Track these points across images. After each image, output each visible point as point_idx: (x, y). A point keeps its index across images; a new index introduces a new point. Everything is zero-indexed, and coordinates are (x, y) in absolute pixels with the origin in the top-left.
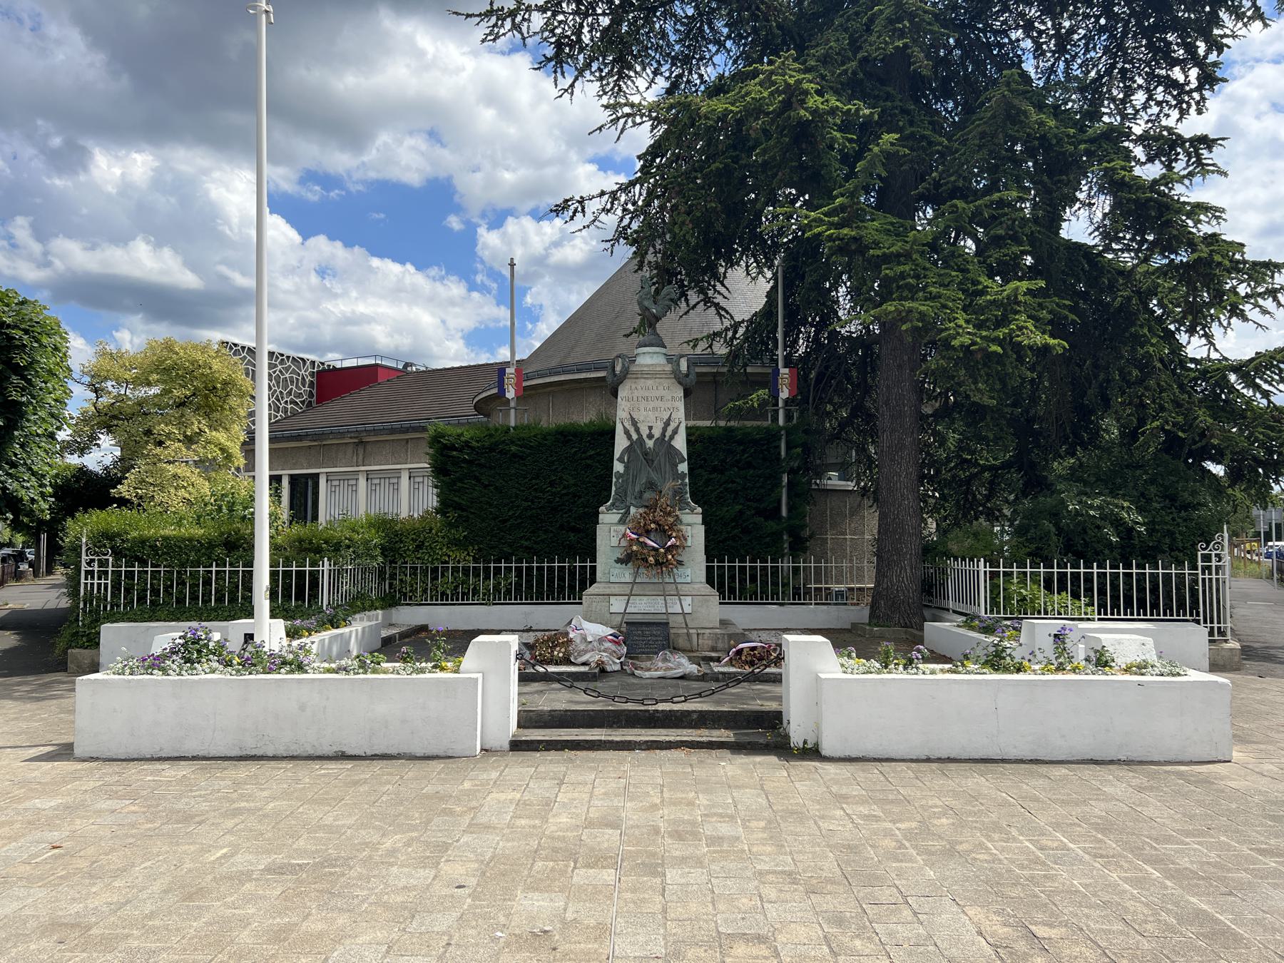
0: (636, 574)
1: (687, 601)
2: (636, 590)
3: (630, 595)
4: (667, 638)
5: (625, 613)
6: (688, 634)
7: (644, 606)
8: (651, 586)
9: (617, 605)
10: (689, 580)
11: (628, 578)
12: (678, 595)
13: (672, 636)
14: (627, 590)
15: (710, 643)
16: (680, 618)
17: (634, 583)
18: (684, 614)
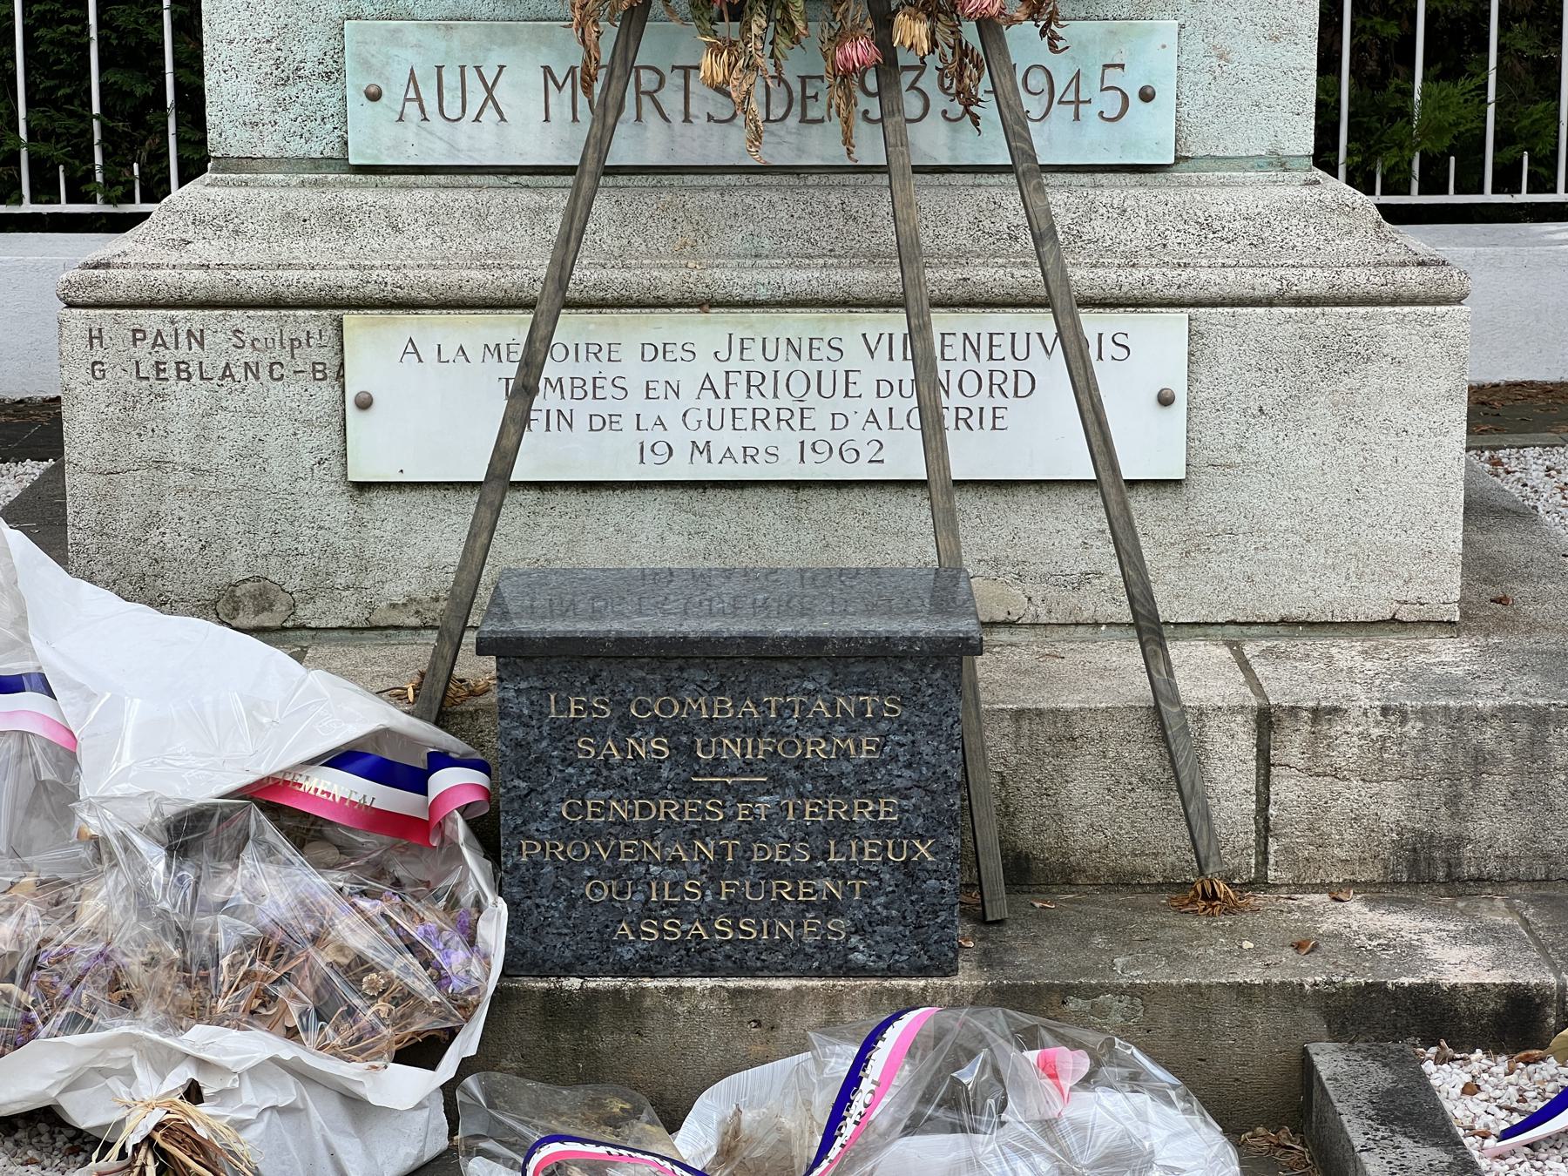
0: (606, 86)
1: (1144, 357)
2: (617, 245)
3: (553, 300)
4: (952, 799)
5: (499, 479)
6: (1164, 720)
7: (721, 420)
8: (777, 206)
9: (424, 404)
10: (1149, 134)
11: (535, 127)
12: (1059, 301)
13: (998, 744)
14: (519, 243)
15: (1391, 806)
16: (1076, 537)
17: (590, 174)
18: (1110, 487)
